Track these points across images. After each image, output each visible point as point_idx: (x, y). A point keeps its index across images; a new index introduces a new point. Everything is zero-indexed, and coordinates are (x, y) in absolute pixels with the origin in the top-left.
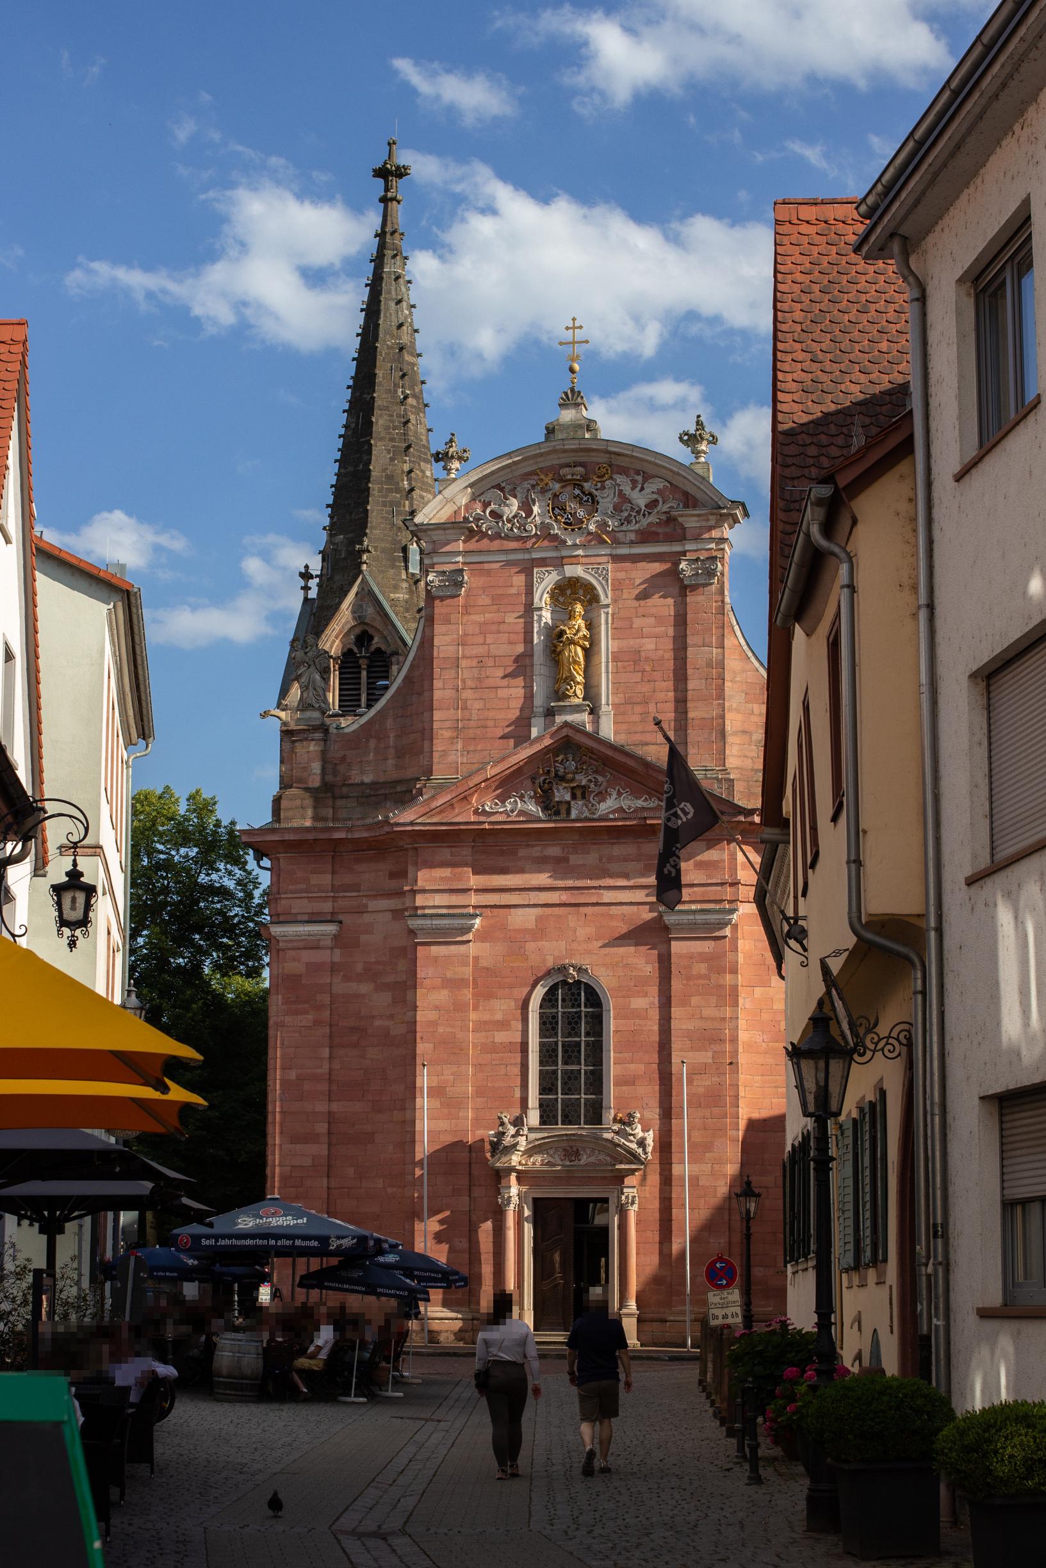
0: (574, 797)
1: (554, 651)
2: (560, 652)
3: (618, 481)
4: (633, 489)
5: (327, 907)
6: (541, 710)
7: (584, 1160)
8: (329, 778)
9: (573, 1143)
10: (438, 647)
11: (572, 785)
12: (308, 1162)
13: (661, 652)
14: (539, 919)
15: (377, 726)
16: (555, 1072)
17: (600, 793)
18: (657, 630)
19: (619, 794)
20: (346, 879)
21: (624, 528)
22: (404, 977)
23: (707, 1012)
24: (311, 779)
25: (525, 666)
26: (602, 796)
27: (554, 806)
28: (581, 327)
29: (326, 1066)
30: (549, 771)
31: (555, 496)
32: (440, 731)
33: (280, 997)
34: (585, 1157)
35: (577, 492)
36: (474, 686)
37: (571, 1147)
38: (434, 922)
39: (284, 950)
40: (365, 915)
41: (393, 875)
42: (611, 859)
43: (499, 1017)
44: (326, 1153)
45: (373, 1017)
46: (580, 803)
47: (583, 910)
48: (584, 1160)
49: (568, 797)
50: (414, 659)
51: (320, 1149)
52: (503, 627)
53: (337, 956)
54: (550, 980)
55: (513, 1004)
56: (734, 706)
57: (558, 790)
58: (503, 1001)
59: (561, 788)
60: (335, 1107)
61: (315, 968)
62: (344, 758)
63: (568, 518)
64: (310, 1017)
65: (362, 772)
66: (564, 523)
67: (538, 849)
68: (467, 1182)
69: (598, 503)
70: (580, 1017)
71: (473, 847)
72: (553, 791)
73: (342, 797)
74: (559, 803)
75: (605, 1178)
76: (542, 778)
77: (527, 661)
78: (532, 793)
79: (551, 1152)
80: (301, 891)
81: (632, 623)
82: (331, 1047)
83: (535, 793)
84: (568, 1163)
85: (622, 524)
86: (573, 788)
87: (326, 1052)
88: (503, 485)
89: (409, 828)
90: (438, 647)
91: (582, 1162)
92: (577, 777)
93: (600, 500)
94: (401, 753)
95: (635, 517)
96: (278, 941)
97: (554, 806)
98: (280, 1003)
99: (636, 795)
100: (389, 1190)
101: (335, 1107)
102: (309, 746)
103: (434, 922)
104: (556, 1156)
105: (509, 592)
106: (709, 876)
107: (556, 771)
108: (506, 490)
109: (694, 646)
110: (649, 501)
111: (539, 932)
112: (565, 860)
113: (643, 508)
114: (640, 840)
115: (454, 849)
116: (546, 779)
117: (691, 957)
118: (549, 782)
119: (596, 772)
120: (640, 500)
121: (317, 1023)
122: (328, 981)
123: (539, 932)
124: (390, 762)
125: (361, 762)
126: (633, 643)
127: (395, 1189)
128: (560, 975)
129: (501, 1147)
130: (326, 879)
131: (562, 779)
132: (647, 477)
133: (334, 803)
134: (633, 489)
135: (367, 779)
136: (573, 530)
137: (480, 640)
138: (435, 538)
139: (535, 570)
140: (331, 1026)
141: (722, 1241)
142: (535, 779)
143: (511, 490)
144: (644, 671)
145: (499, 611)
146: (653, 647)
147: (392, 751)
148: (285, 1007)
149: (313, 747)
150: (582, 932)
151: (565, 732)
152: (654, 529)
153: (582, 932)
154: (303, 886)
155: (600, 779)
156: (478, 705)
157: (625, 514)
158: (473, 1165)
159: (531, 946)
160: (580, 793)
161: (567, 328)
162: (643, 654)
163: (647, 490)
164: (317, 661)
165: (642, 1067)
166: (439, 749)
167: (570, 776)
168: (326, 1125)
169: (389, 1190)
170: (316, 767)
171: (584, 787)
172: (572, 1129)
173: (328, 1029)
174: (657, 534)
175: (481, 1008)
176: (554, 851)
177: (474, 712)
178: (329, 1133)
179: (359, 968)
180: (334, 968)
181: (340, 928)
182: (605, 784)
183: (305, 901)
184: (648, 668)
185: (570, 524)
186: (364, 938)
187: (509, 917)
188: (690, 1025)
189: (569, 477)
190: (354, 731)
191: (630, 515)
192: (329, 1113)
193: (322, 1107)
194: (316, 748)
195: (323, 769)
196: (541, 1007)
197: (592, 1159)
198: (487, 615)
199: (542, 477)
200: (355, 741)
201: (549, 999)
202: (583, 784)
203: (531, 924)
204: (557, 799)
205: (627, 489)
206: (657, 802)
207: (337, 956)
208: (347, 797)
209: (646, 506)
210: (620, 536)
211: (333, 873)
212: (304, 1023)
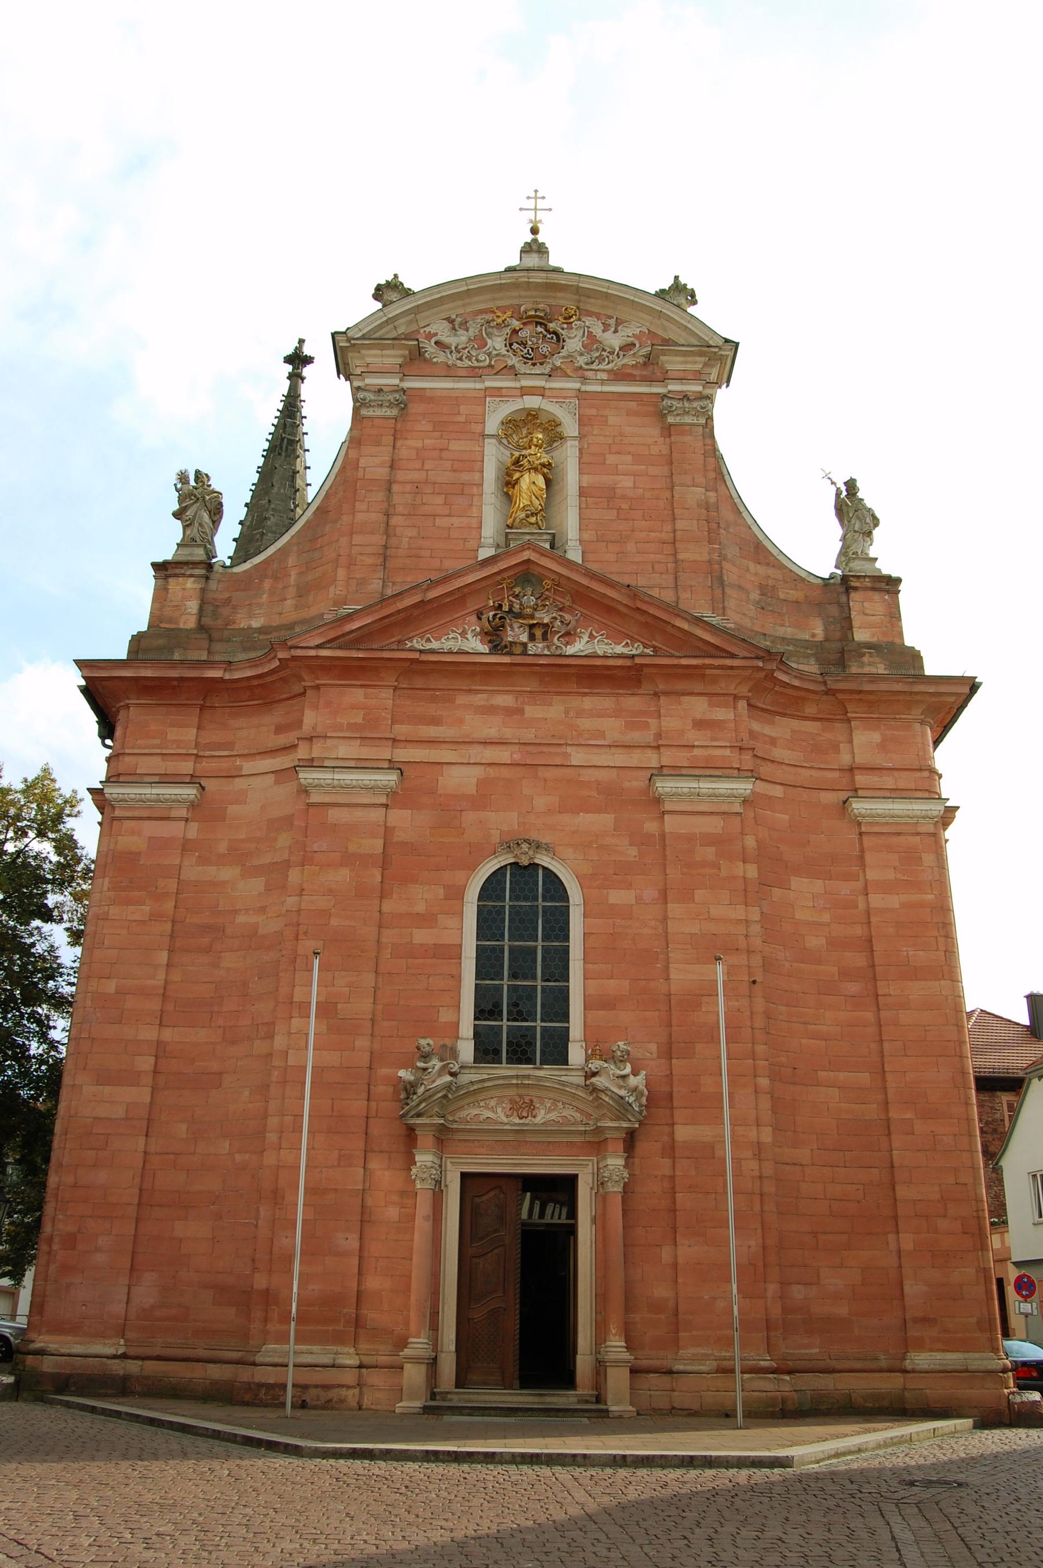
0: (532, 637)
1: (508, 484)
2: (517, 481)
3: (587, 323)
4: (603, 331)
5: (187, 767)
6: (491, 541)
7: (541, 1116)
8: (207, 621)
9: (522, 1091)
10: (364, 469)
11: (532, 622)
12: (120, 1112)
13: (641, 491)
14: (482, 783)
15: (275, 565)
16: (514, 976)
17: (568, 634)
18: (636, 468)
19: (591, 637)
20: (213, 735)
21: (594, 366)
22: (286, 856)
23: (716, 911)
24: (182, 620)
25: (473, 495)
26: (569, 636)
27: (506, 647)
28: (544, 198)
29: (161, 976)
30: (500, 606)
31: (515, 332)
32: (360, 557)
33: (107, 880)
34: (543, 1112)
35: (539, 329)
36: (406, 512)
37: (521, 1096)
38: (337, 776)
39: (120, 819)
40: (237, 780)
41: (279, 729)
42: (580, 713)
43: (420, 908)
44: (148, 1100)
45: (235, 912)
46: (540, 645)
47: (542, 772)
48: (541, 1116)
49: (524, 638)
50: (331, 488)
51: (142, 1095)
52: (445, 454)
53: (193, 831)
54: (496, 861)
55: (441, 892)
56: (729, 556)
57: (512, 629)
58: (427, 888)
59: (516, 626)
60: (167, 1034)
61: (159, 845)
62: (228, 601)
63: (528, 353)
64: (146, 908)
65: (251, 616)
66: (523, 356)
67: (485, 696)
68: (362, 1145)
69: (564, 341)
70: (537, 913)
71: (395, 688)
72: (506, 631)
73: (220, 640)
74: (511, 643)
75: (571, 1144)
76: (491, 614)
77: (475, 490)
78: (478, 629)
79: (493, 1103)
80: (154, 747)
81: (605, 459)
82: (171, 951)
83: (482, 629)
84: (517, 1121)
85: (592, 363)
86: (532, 627)
87: (165, 954)
88: (454, 317)
89: (312, 653)
90: (364, 469)
91: (538, 1120)
92: (537, 615)
93: (567, 340)
94: (303, 592)
95: (608, 357)
96: (113, 808)
97: (506, 647)
98: (105, 889)
99: (616, 636)
100: (238, 1157)
101: (167, 1034)
102: (184, 584)
103: (337, 776)
104: (499, 1110)
105: (455, 420)
106: (713, 739)
107: (511, 606)
108: (456, 323)
109: (681, 485)
110: (624, 343)
111: (480, 800)
112: (520, 711)
113: (617, 349)
114: (621, 691)
115: (369, 690)
116: (495, 615)
117: (690, 838)
118: (501, 618)
119: (561, 610)
120: (614, 340)
121: (155, 917)
122: (177, 862)
123: (480, 800)
124: (289, 602)
125: (249, 604)
126: (607, 480)
127: (247, 1156)
128: (510, 855)
129: (421, 1090)
130: (190, 734)
131: (519, 616)
132: (619, 322)
133: (210, 645)
134: (603, 331)
135: (256, 624)
136: (534, 365)
137: (418, 465)
138: (369, 360)
139: (488, 399)
140: (173, 922)
141: (753, 1243)
142: (482, 614)
143: (461, 324)
144: (619, 509)
145: (441, 437)
146: (631, 485)
147: (292, 591)
148: (111, 894)
149: (190, 584)
150: (541, 802)
151: (526, 555)
152: (629, 371)
153: (541, 802)
154: (157, 741)
155: (568, 617)
156: (412, 532)
157: (597, 354)
158: (371, 1121)
159: (470, 817)
160: (543, 631)
161: (528, 198)
162: (618, 491)
163: (620, 334)
165: (626, 983)
166: (358, 576)
167: (528, 611)
168: (152, 1060)
169: (238, 1157)
170: (193, 606)
171: (547, 625)
172: (525, 1069)
173: (170, 924)
174: (634, 376)
175: (395, 896)
176: (505, 700)
177: (405, 540)
178: (155, 1072)
179: (223, 847)
180: (186, 846)
181: (201, 795)
182: (573, 623)
183: (158, 759)
184: (624, 507)
185: (532, 359)
186: (232, 809)
187: (440, 778)
188: (694, 928)
189: (532, 313)
190: (245, 571)
191: (601, 355)
192: (159, 1042)
193: (149, 1033)
194: (195, 586)
195: (201, 609)
196: (479, 900)
197: (553, 1116)
198: (427, 442)
199: (499, 314)
200: (246, 582)
201: (491, 888)
202: (545, 621)
203: (472, 790)
204: (510, 639)
205: (597, 330)
206: (641, 647)
207: (193, 831)
208: (229, 641)
209: (620, 349)
210: (589, 374)
211: (199, 728)
212: (137, 917)
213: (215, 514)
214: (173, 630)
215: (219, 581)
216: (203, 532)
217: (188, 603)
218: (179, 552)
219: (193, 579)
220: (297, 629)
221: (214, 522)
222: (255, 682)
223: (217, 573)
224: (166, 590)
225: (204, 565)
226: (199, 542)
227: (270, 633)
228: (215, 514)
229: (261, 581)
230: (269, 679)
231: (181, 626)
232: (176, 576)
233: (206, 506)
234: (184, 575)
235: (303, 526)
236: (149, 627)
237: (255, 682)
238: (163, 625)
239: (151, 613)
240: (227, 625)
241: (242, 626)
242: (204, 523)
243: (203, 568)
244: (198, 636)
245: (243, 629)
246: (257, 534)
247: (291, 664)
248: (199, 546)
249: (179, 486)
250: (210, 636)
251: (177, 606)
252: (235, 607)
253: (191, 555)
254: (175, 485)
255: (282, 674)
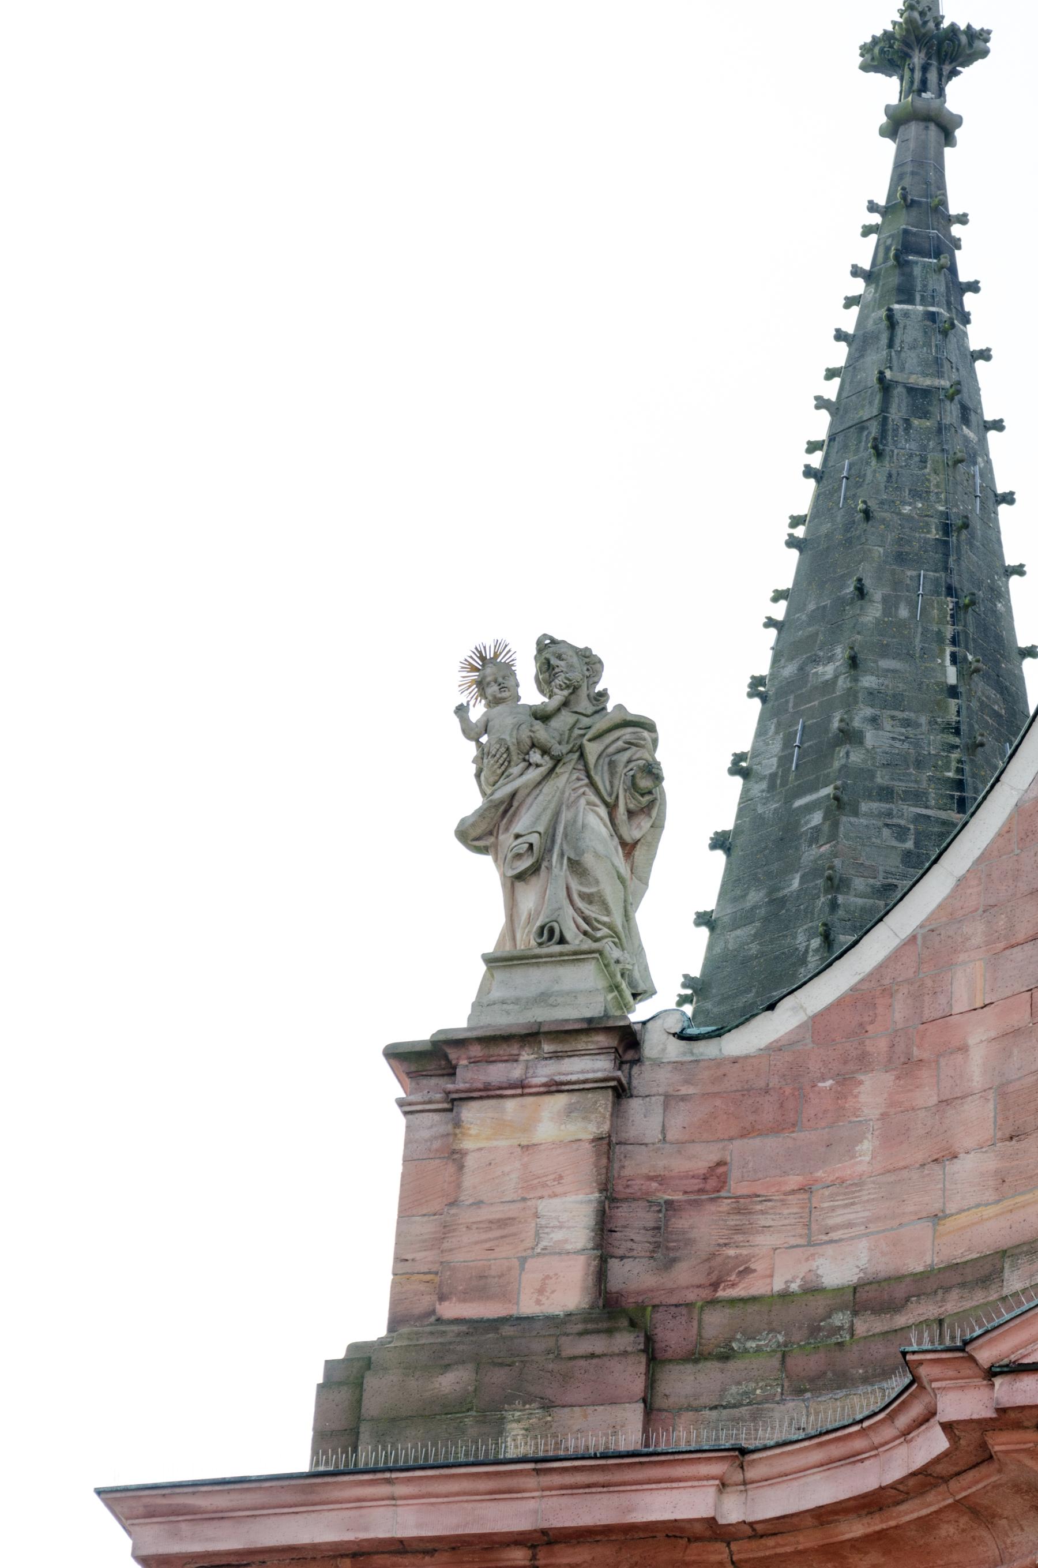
15: (900, 1011)
24: (530, 1279)
73: (695, 1357)
125: (805, 1189)
133: (651, 1383)
164: (592, 750)
190: (775, 1048)
208: (725, 1357)
213: (631, 814)
214: (494, 1324)
215: (669, 1100)
216: (588, 898)
217: (549, 1208)
218: (496, 994)
219: (560, 1101)
220: (1014, 1281)
221: (629, 848)
222: (855, 1529)
223: (658, 1063)
224: (455, 1157)
225: (602, 1040)
226: (575, 940)
227: (893, 1307)
228: (631, 814)
229: (846, 1081)
230: (910, 1512)
231: (527, 1306)
232: (489, 1093)
233: (592, 784)
234: (521, 1088)
235: (1006, 832)
236: (395, 1322)
237: (855, 1529)
238: (450, 1310)
239: (400, 1259)
240: (715, 1286)
241: (778, 1285)
242: (588, 860)
243: (602, 1051)
244: (596, 1344)
245: (785, 1296)
246: (809, 808)
247: (1000, 1443)
248: (578, 956)
249: (477, 712)
250: (649, 1340)
251: (502, 1223)
252: (743, 1206)
253: (543, 998)
254: (461, 711)
255: (968, 1486)
